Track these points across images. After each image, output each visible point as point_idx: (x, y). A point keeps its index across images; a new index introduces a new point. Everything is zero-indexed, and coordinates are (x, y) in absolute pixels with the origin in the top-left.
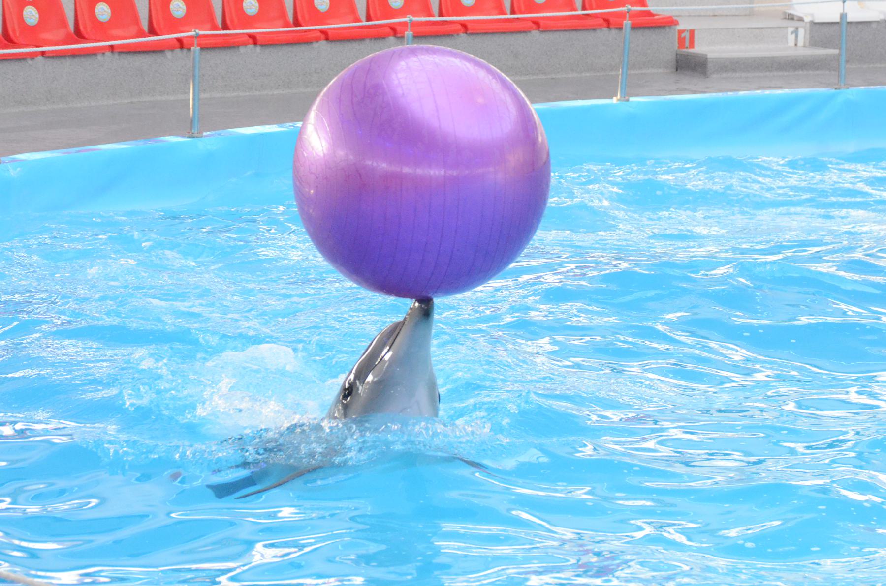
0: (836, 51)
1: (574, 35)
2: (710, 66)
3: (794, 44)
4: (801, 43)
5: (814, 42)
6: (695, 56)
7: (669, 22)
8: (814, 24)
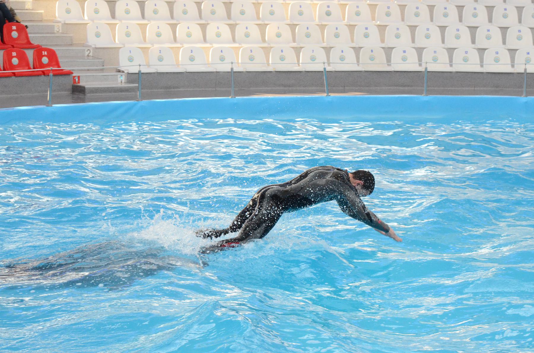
0: (137, 85)
1: (30, 78)
2: (86, 91)
3: (121, 81)
4: (123, 81)
5: (129, 81)
6: (80, 87)
7: (69, 73)
8: (128, 73)
